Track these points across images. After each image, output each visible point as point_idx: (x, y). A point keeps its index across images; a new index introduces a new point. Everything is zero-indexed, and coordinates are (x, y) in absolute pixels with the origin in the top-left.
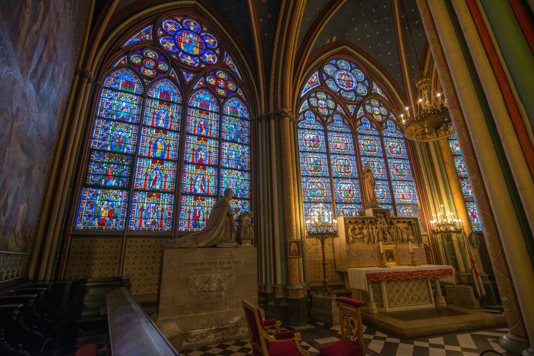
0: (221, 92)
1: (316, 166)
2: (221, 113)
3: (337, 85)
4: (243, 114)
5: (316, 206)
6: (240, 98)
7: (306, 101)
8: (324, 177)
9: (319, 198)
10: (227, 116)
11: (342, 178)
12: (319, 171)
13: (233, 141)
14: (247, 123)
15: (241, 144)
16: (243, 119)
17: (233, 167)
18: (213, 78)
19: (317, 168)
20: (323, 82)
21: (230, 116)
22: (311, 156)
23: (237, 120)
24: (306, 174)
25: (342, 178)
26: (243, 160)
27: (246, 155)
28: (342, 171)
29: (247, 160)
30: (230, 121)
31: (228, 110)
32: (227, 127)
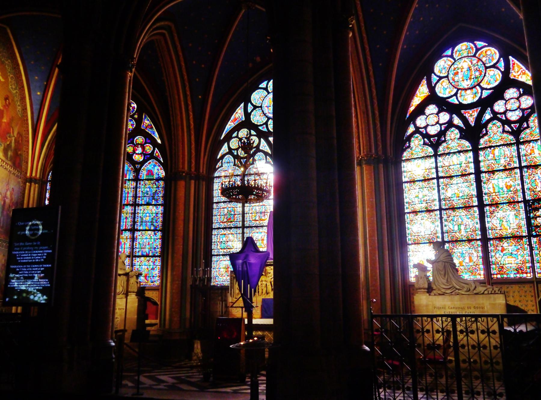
0: (138, 158)
1: (229, 217)
2: (137, 179)
3: (265, 115)
4: (158, 174)
5: (224, 259)
6: (156, 159)
7: (226, 144)
8: (236, 227)
9: (229, 250)
10: (143, 180)
11: (257, 227)
12: (231, 222)
13: (148, 204)
14: (162, 183)
15: (155, 205)
16: (158, 179)
17: (147, 228)
18: (131, 146)
19: (230, 219)
20: (248, 115)
21: (146, 180)
22: (225, 206)
23: (152, 182)
24: (218, 226)
25: (257, 227)
26: (156, 220)
27: (160, 215)
28: (257, 219)
29: (160, 219)
30: (146, 185)
31: (143, 174)
32: (142, 192)
